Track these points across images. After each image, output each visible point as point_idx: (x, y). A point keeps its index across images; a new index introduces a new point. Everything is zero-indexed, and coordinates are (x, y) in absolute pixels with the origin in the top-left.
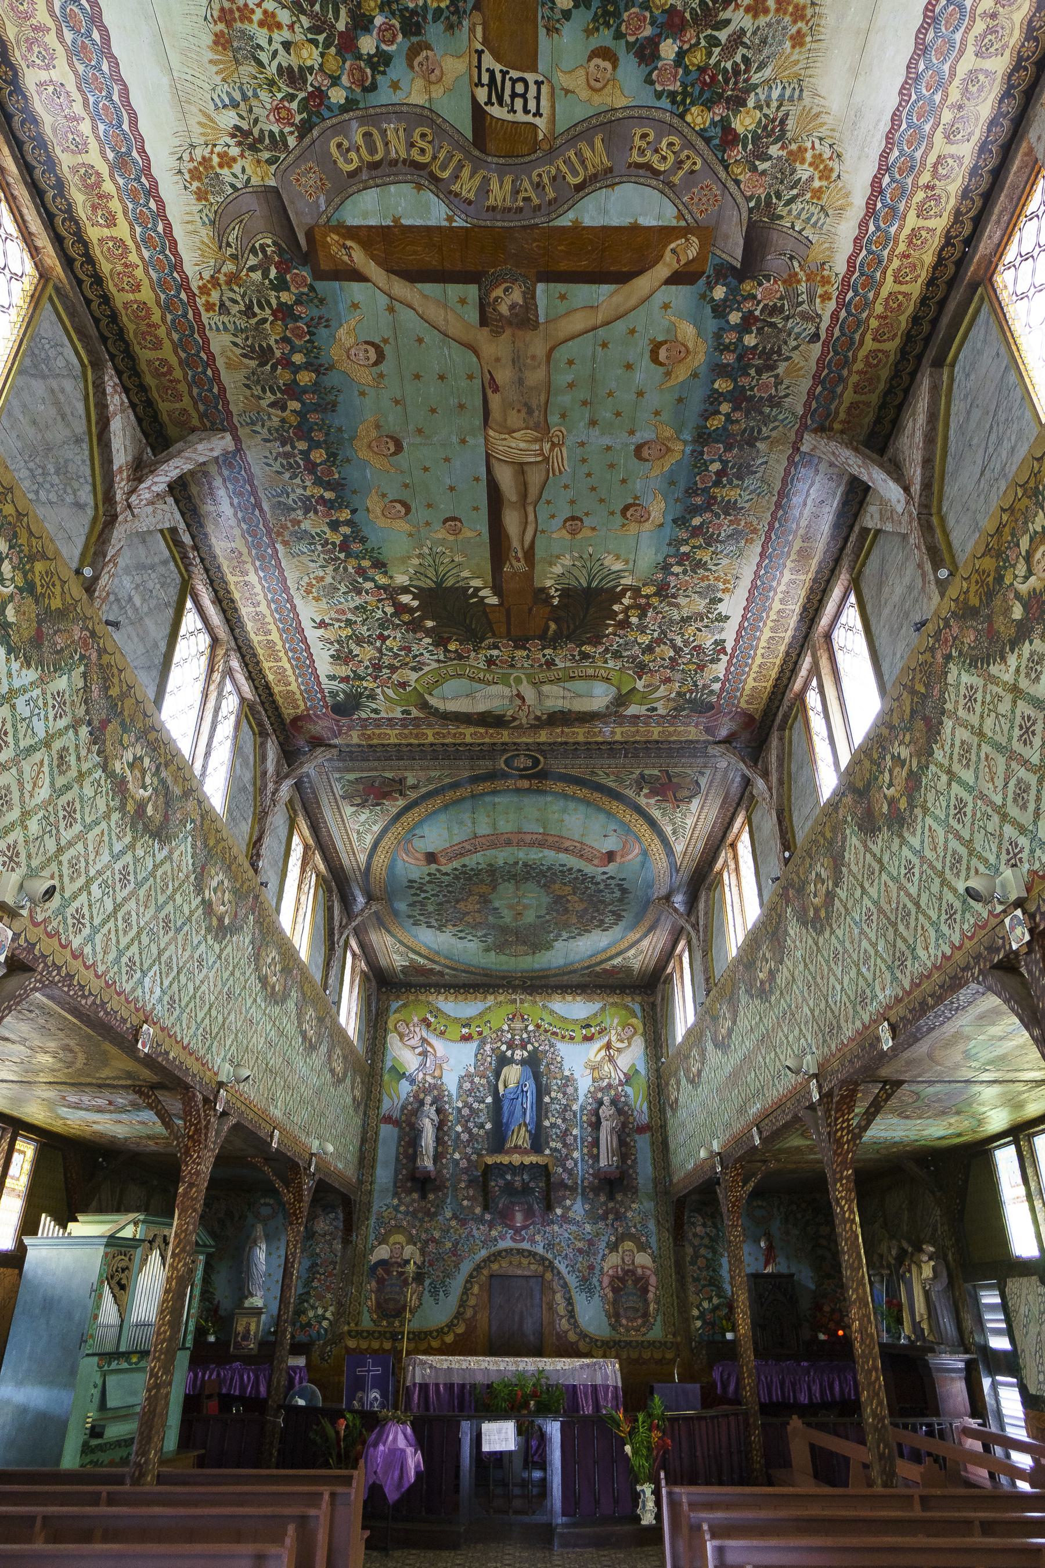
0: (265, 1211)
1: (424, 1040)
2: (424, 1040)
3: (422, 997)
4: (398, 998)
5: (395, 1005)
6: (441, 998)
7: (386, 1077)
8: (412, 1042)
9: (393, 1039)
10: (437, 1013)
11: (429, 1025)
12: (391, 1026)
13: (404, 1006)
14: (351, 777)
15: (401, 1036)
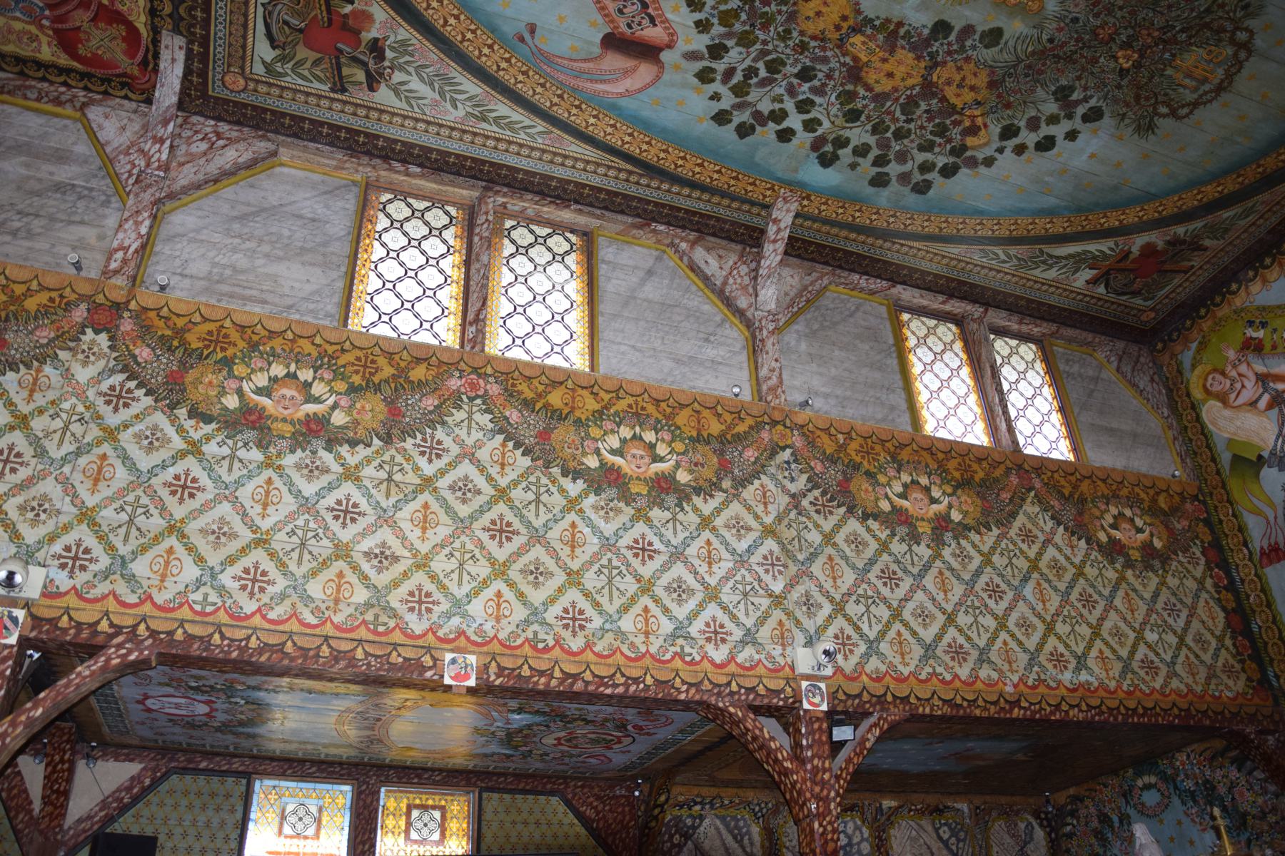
0: (1151, 798)
1: (1263, 379)
2: (1263, 379)
3: (1223, 311)
4: (1187, 341)
5: (1187, 357)
6: (1255, 287)
7: (1234, 485)
8: (1246, 396)
9: (1212, 412)
10: (1262, 317)
11: (1255, 347)
12: (1197, 394)
13: (1203, 346)
14: (264, 51)
15: (1223, 398)
